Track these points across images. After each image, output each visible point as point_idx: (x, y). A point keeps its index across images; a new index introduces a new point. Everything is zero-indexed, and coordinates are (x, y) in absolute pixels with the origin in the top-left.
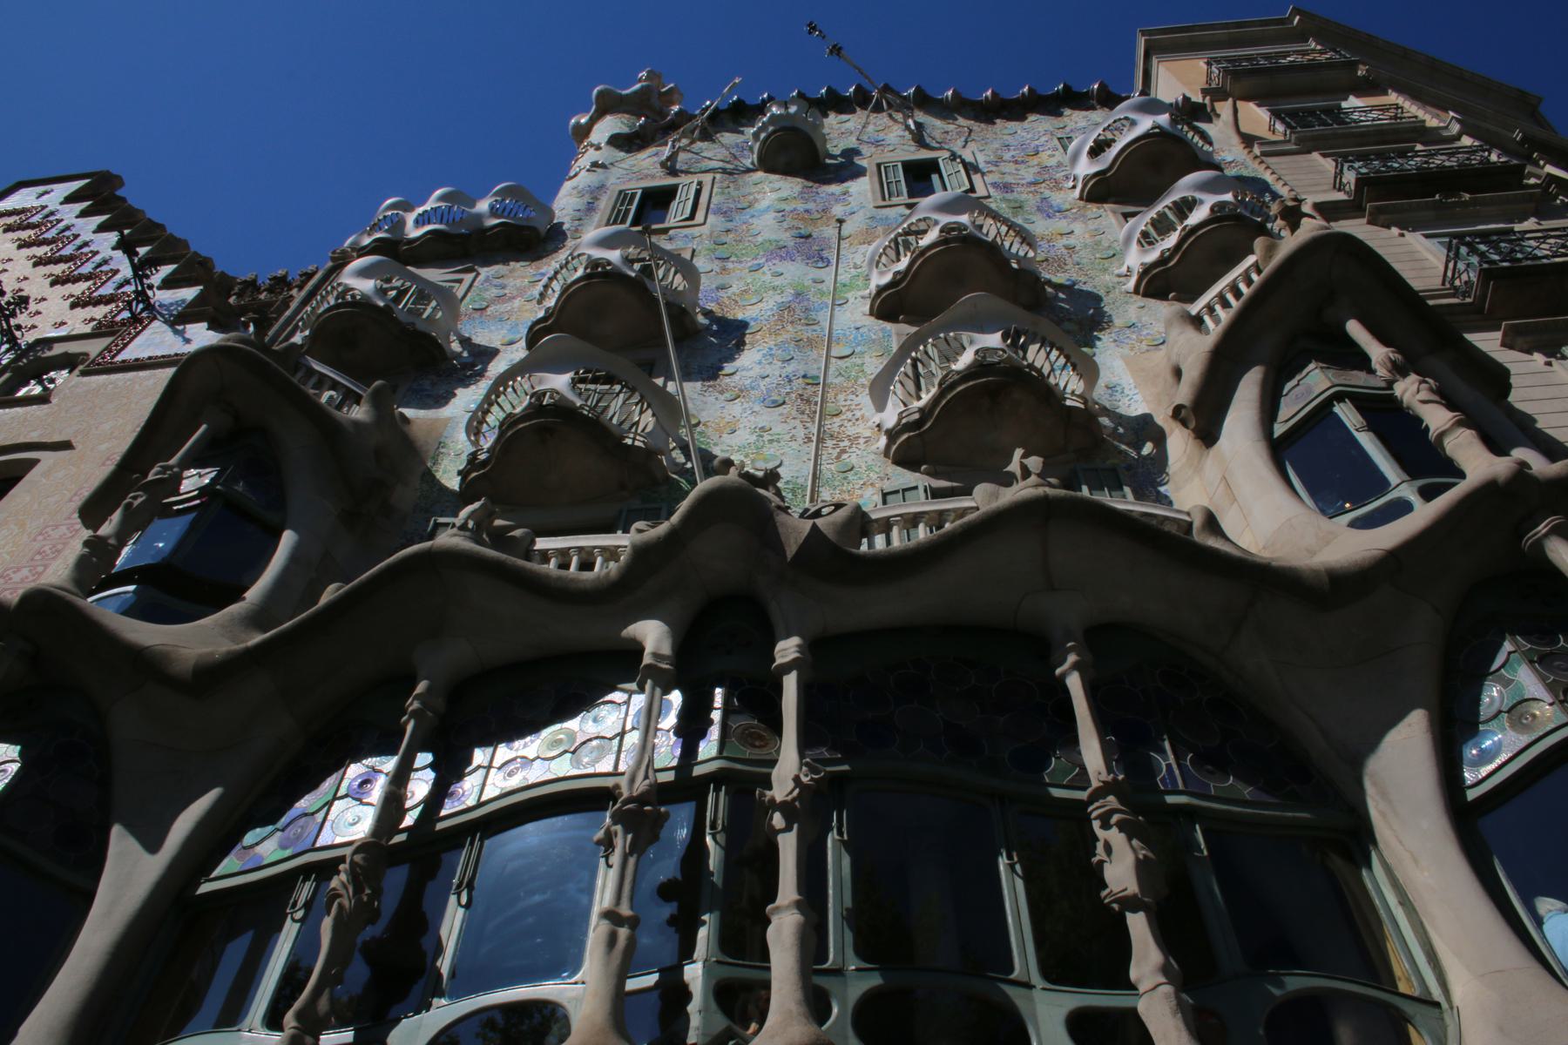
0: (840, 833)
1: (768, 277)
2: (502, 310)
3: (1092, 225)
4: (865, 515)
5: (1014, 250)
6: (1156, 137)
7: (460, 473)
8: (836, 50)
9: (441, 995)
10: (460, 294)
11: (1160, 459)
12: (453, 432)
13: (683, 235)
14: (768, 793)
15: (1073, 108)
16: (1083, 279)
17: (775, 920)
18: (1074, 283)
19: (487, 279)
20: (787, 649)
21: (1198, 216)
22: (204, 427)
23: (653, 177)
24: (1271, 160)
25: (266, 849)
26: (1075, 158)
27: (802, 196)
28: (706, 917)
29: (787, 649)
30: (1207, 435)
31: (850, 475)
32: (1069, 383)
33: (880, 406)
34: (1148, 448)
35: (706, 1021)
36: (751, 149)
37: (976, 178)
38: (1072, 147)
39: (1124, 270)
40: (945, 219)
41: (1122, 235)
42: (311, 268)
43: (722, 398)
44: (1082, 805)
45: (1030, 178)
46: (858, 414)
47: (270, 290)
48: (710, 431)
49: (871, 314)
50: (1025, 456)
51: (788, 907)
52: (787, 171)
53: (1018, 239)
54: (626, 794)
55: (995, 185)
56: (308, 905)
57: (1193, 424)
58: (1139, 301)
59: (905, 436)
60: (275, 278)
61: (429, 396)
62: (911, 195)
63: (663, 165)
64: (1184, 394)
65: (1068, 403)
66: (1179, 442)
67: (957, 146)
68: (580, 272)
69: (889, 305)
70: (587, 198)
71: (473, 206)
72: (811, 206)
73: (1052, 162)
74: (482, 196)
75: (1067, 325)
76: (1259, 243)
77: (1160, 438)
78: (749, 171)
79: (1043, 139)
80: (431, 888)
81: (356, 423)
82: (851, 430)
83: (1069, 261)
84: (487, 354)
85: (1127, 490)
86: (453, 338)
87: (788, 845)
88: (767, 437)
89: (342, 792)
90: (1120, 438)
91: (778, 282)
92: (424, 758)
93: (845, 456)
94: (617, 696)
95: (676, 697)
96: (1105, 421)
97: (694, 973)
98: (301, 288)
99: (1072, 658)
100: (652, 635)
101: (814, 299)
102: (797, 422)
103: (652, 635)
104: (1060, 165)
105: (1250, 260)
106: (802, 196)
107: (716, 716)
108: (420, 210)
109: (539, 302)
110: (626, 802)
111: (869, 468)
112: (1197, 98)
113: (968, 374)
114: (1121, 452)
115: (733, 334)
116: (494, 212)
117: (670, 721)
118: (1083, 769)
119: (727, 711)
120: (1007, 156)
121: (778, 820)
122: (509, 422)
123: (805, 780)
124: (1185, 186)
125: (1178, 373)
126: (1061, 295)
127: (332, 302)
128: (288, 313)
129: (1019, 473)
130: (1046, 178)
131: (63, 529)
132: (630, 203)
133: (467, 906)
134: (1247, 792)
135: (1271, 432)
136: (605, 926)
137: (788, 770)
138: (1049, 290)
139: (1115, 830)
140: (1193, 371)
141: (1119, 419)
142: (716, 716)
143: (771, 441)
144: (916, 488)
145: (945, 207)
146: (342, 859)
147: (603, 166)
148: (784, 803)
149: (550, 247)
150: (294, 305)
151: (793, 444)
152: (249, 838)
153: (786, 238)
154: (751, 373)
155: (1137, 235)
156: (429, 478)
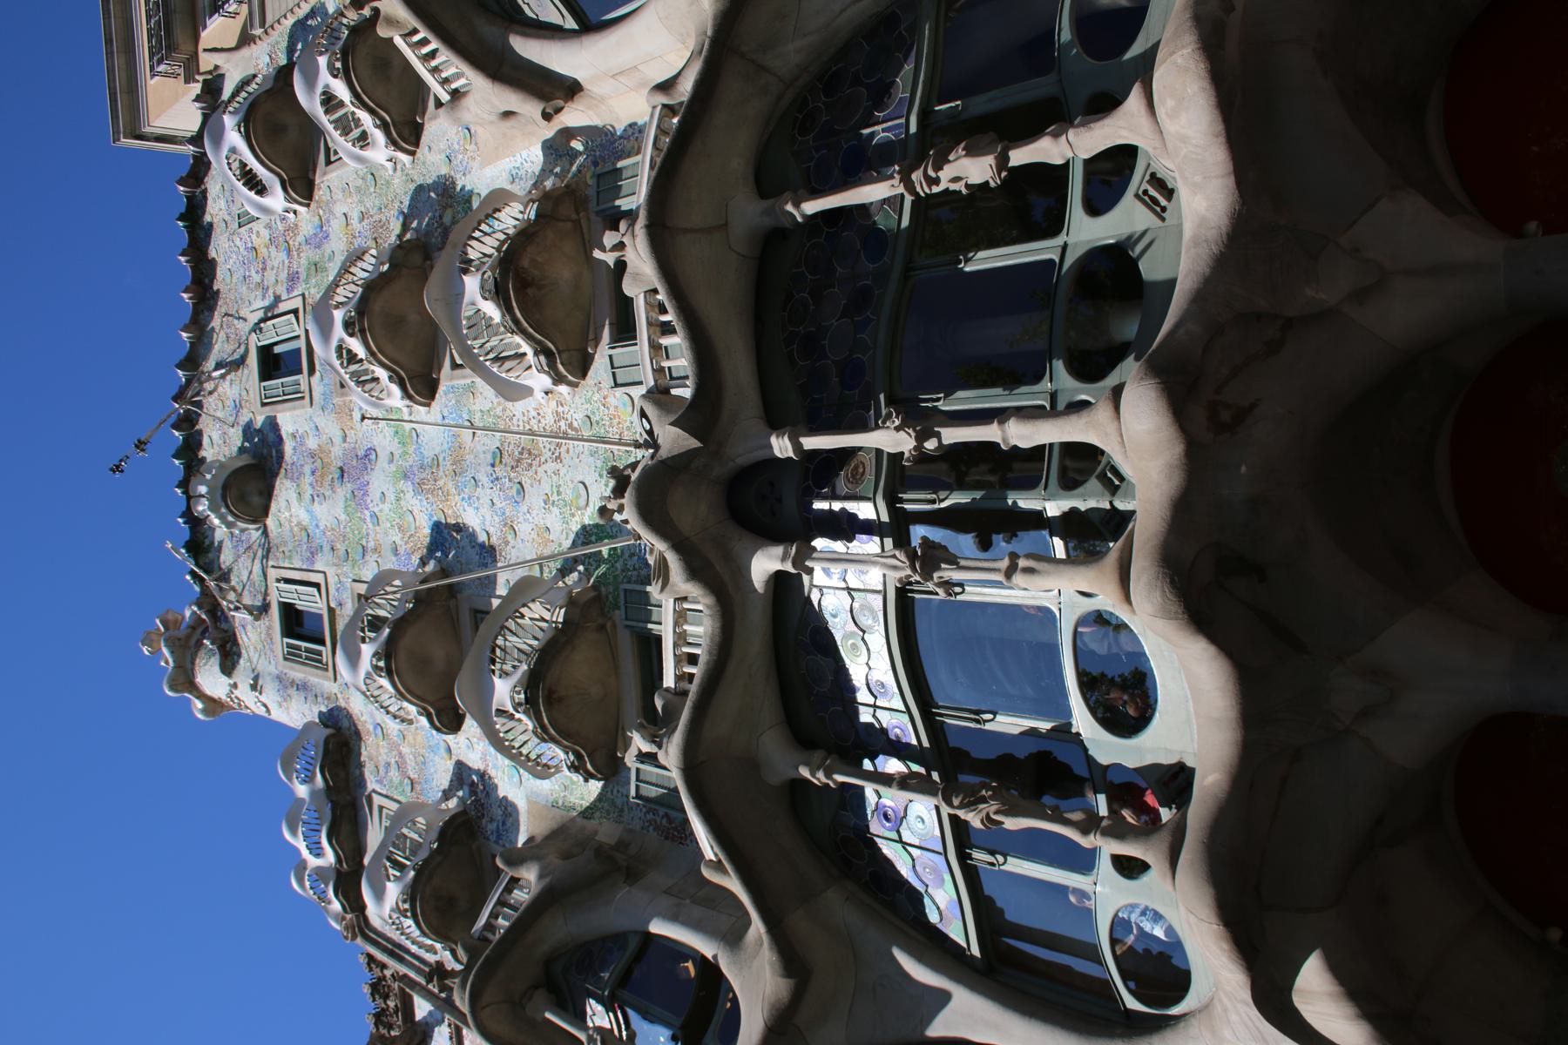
0: (938, 400)
1: (386, 507)
2: (415, 764)
3: (338, 195)
4: (649, 392)
5: (370, 268)
6: (248, 127)
7: (586, 780)
8: (140, 445)
9: (1070, 725)
10: (394, 806)
11: (588, 132)
12: (543, 790)
13: (337, 590)
14: (907, 455)
15: (204, 212)
16: (397, 205)
17: (1014, 442)
19: (380, 782)
20: (781, 447)
21: (341, 90)
22: (548, 1015)
23: (269, 628)
24: (269, 19)
25: (944, 902)
26: (265, 210)
27: (296, 478)
28: (1010, 502)
29: (781, 447)
30: (571, 89)
31: (594, 419)
32: (510, 219)
33: (528, 391)
34: (577, 145)
35: (1092, 495)
36: (243, 531)
37: (283, 307)
39: (389, 165)
40: (339, 332)
41: (352, 164)
42: (362, 960)
43: (512, 542)
44: (918, 202)
45: (283, 256)
46: (533, 413)
47: (386, 997)
49: (428, 405)
50: (603, 249)
51: (1003, 431)
52: (268, 494)
53: (360, 264)
54: (909, 572)
55: (289, 291)
56: (992, 853)
57: (560, 103)
58: (422, 151)
59: (560, 367)
60: (372, 994)
61: (504, 823)
62: (300, 372)
63: (257, 618)
64: (530, 108)
65: (532, 216)
66: (574, 116)
67: (244, 328)
68: (385, 682)
69: (422, 386)
70: (292, 691)
71: (303, 800)
72: (307, 470)
73: (265, 233)
74: (291, 792)
75: (447, 219)
76: (383, 31)
77: (568, 133)
78: (265, 533)
79: (238, 242)
80: (979, 753)
81: (541, 877)
83: (377, 218)
84: (462, 772)
85: (619, 165)
86: (443, 806)
87: (953, 435)
88: (555, 497)
89: (894, 835)
90: (565, 171)
91: (391, 497)
92: (867, 765)
93: (575, 424)
94: (815, 596)
95: (820, 543)
96: (548, 184)
97: (1053, 509)
98: (384, 966)
99: (789, 208)
100: (765, 564)
101: (411, 460)
103: (765, 564)
106: (296, 478)
107: (837, 506)
108: (305, 853)
109: (411, 722)
110: (914, 569)
111: (589, 401)
112: (197, 88)
113: (507, 308)
114: (579, 171)
115: (445, 536)
116: (308, 780)
117: (839, 546)
118: (885, 201)
119: (834, 497)
120: (257, 278)
121: (931, 445)
122: (544, 735)
123: (897, 423)
124: (310, 103)
125: (508, 114)
126: (414, 225)
127: (410, 922)
128: (412, 975)
129: (617, 254)
130: (284, 240)
132: (299, 648)
133: (995, 714)
134: (908, 67)
135: (574, 31)
136: (1018, 579)
137: (892, 439)
138: (408, 236)
139: (941, 174)
140: (510, 99)
141: (545, 171)
142: (837, 506)
143: (559, 493)
145: (326, 332)
146: (954, 819)
147: (256, 679)
148: (917, 439)
149: (345, 723)
150: (403, 970)
152: (933, 917)
153: (343, 491)
154: (488, 517)
155: (357, 150)
156: (587, 813)
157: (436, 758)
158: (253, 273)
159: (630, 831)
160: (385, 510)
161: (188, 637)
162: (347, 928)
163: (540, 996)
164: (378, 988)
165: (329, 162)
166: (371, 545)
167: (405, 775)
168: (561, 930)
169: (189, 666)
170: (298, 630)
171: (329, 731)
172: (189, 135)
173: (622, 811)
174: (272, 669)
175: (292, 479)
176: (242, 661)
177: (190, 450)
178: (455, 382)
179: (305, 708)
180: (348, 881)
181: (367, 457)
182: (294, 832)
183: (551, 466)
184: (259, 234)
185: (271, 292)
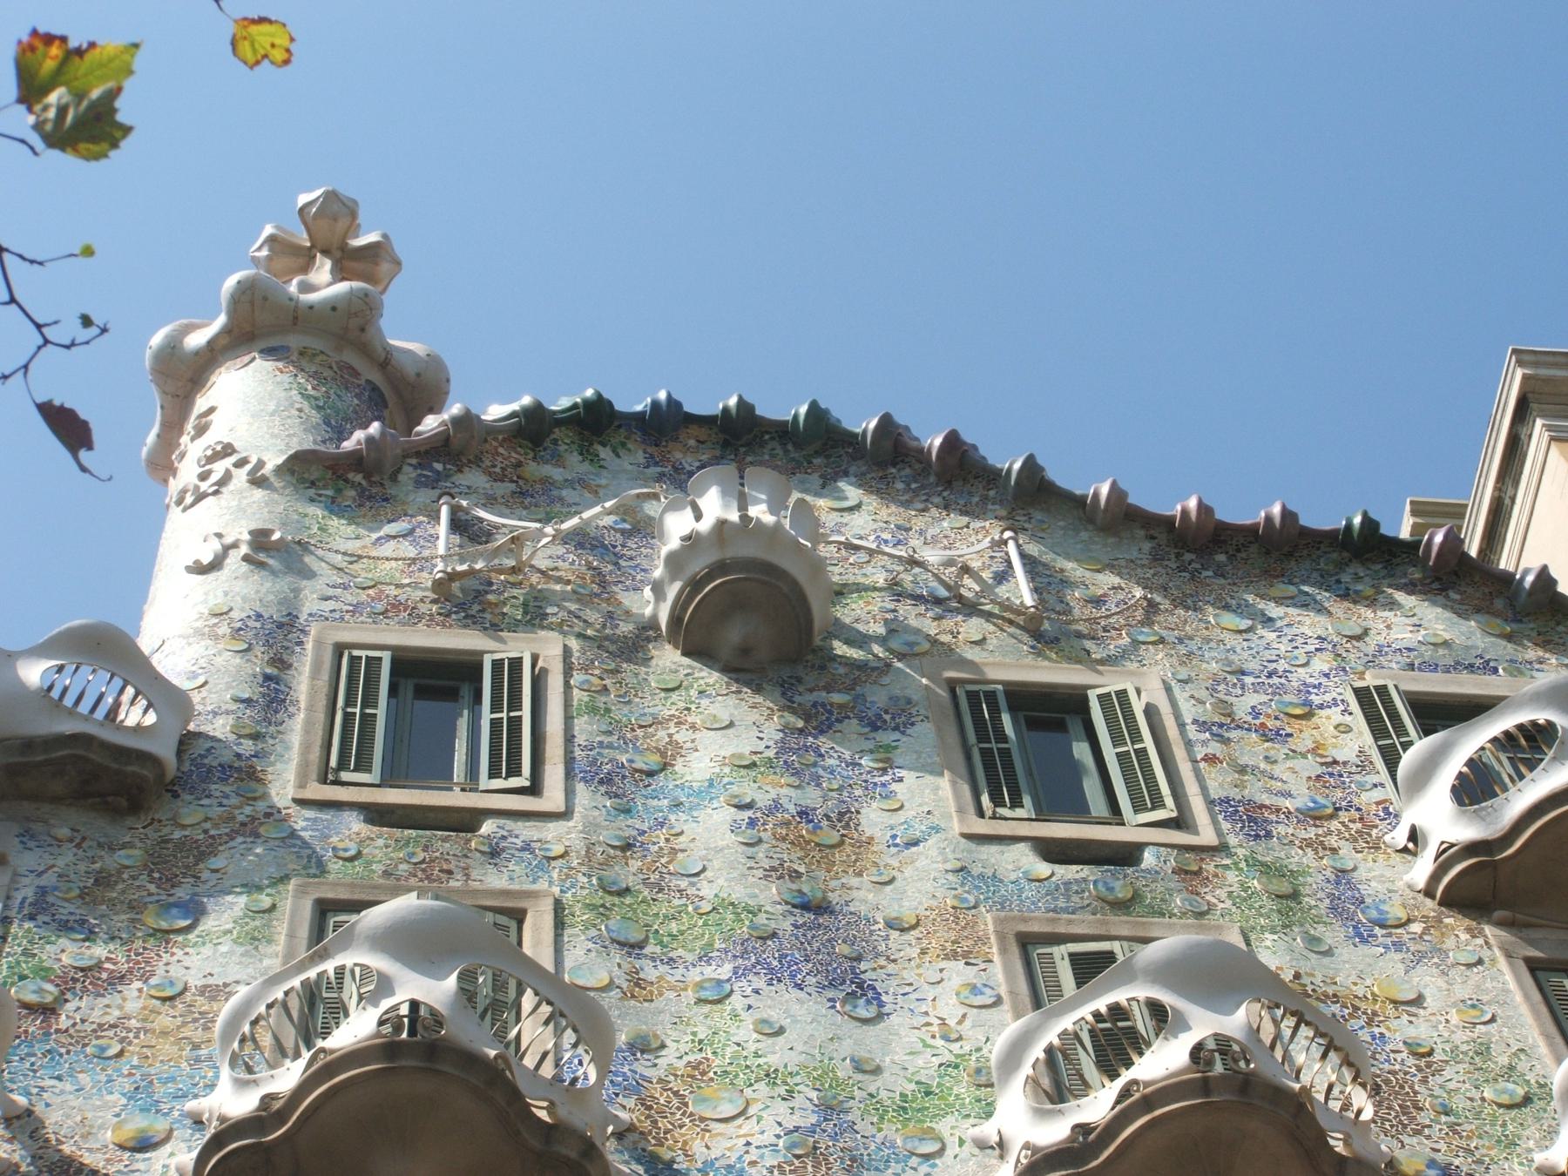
1: (745, 1032)
45: (1302, 797)
52: (744, 670)
70: (258, 664)
72: (810, 796)
79: (1321, 664)
83: (1424, 1099)
91: (777, 1055)
104: (1364, 765)
120: (1243, 705)
132: (370, 700)
158: (1253, 699)
161: (365, 349)
165: (1534, 966)
166: (650, 972)
169: (294, 341)
174: (310, 603)
175: (783, 748)
176: (316, 511)
181: (855, 989)
185: (1215, 748)
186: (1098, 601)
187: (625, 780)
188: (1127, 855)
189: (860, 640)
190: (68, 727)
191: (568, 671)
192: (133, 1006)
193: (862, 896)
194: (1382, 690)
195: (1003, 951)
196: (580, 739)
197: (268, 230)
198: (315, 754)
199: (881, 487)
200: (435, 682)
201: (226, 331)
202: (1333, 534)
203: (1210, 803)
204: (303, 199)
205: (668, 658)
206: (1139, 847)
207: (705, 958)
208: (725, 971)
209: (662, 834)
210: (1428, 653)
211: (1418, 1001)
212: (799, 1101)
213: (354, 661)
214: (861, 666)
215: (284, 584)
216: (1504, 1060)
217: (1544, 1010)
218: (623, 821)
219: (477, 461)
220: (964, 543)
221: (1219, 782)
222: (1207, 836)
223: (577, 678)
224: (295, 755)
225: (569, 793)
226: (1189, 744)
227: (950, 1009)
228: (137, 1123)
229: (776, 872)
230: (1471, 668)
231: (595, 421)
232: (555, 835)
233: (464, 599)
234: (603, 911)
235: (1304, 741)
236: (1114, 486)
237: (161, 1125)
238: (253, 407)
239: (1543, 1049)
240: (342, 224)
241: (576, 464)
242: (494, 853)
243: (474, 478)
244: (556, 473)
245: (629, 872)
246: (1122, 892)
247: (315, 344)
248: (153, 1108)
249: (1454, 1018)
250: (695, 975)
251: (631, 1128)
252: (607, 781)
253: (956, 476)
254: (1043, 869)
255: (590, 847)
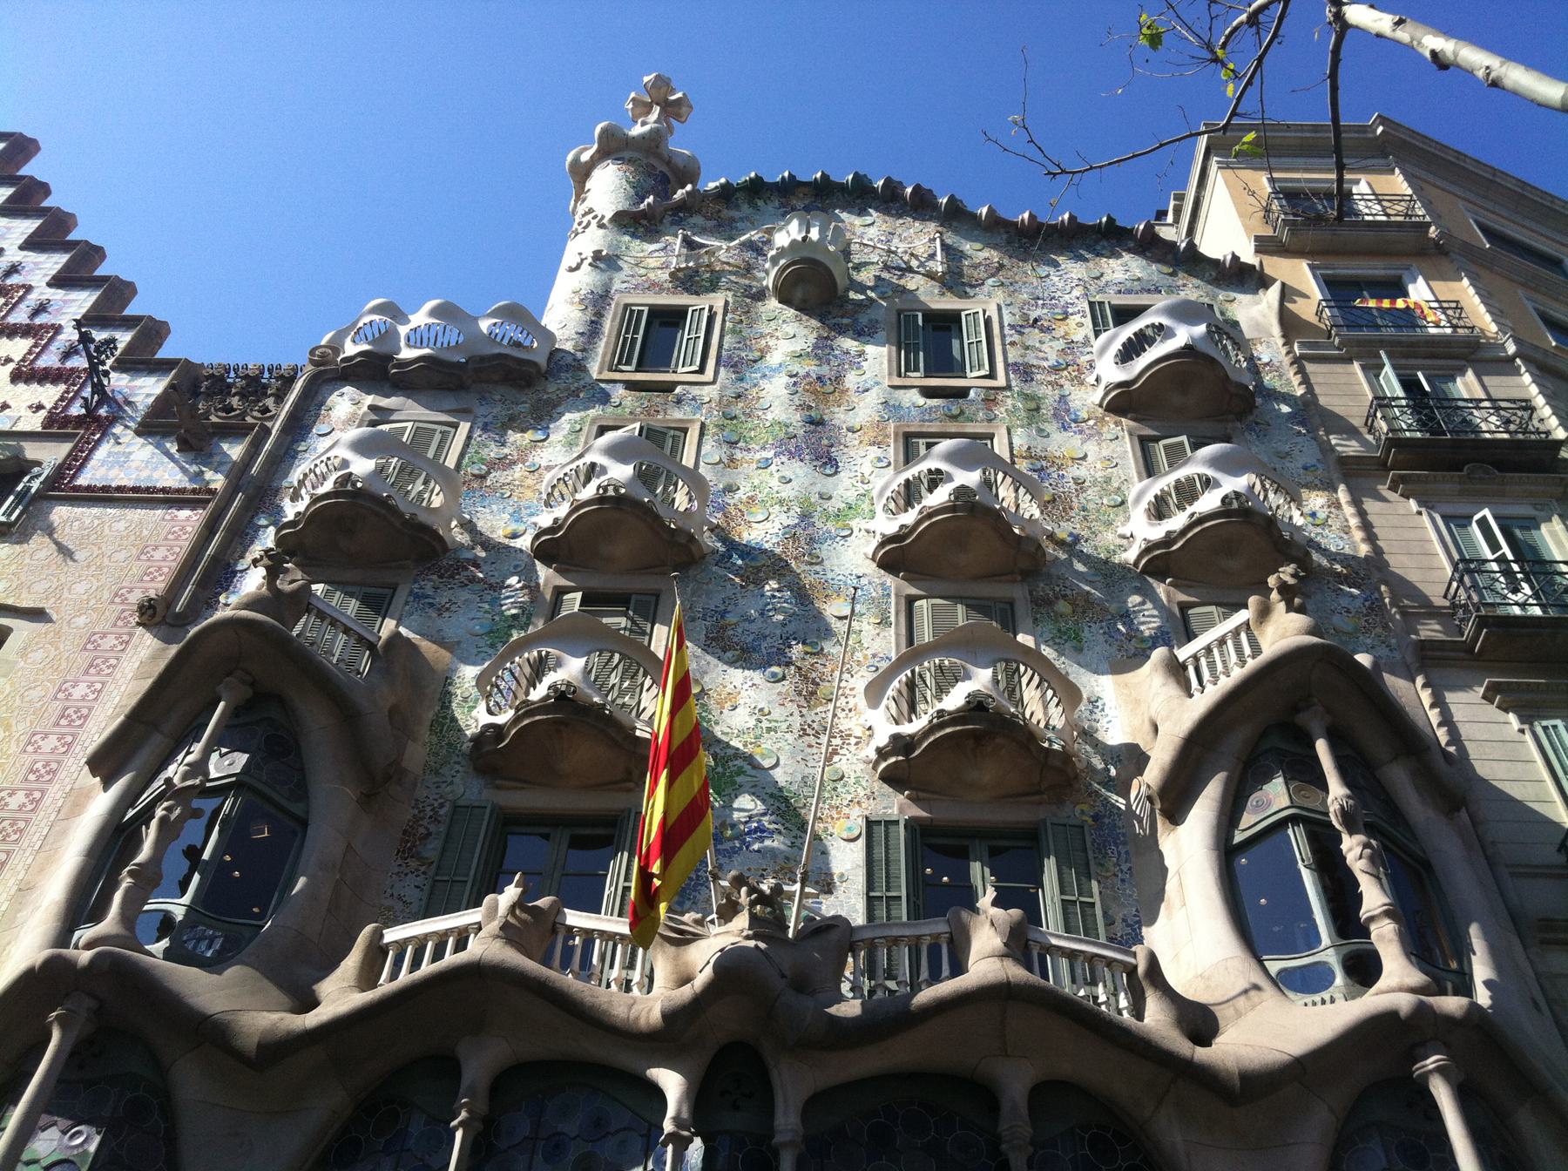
1: (774, 483)
18: (1077, 539)
21: (1209, 502)
24: (1310, 367)
31: (839, 785)
38: (1104, 337)
45: (1052, 362)
46: (852, 702)
47: (243, 395)
48: (712, 704)
49: (873, 559)
52: (804, 308)
59: (893, 760)
61: (431, 605)
68: (589, 492)
70: (589, 316)
73: (1078, 336)
76: (1253, 600)
82: (844, 724)
83: (1075, 505)
86: (454, 523)
88: (765, 724)
91: (787, 492)
93: (836, 758)
98: (280, 398)
102: (793, 707)
104: (1086, 343)
105: (1242, 616)
112: (1248, 256)
113: (957, 717)
125: (1156, 729)
131: (53, 741)
132: (636, 331)
143: (769, 730)
144: (897, 822)
150: (276, 427)
151: (788, 736)
157: (506, 516)
159: (415, 784)
160: (770, 481)
161: (659, 156)
162: (323, 356)
163: (247, 692)
164: (255, 386)
166: (739, 455)
167: (493, 465)
168: (316, 723)
169: (627, 155)
170: (656, 323)
171: (542, 360)
172: (1197, 241)
173: (437, 773)
174: (617, 285)
175: (816, 347)
176: (627, 238)
177: (860, 196)
178: (893, 600)
179: (570, 332)
180: (375, 371)
182: (434, 313)
183: (797, 721)
184: (1078, 325)
185: (1016, 338)
186: (975, 266)
187: (741, 364)
188: (962, 393)
189: (861, 288)
190: (497, 351)
191: (725, 314)
192: (517, 475)
193: (839, 417)
194: (1101, 303)
195: (896, 441)
196: (726, 346)
197: (633, 95)
198: (608, 358)
199: (886, 211)
200: (668, 320)
201: (598, 151)
202: (1093, 226)
203: (1007, 365)
204: (646, 79)
205: (773, 303)
206: (969, 388)
207: (763, 448)
208: (770, 454)
209: (755, 390)
210: (1129, 284)
211: (1084, 458)
212: (792, 513)
213: (632, 312)
214: (859, 304)
215: (605, 276)
216: (1116, 485)
217: (1141, 461)
218: (740, 384)
219: (699, 212)
220: (919, 240)
221: (1014, 354)
222: (1001, 381)
223: (729, 316)
224: (599, 359)
225: (716, 373)
226: (1003, 336)
227: (867, 469)
228: (513, 527)
229: (804, 407)
230: (1149, 291)
231: (756, 189)
232: (709, 393)
233: (687, 281)
234: (722, 427)
235: (1059, 332)
236: (990, 210)
237: (521, 528)
238: (608, 188)
239: (1136, 479)
240: (664, 90)
241: (746, 209)
242: (679, 401)
243: (698, 220)
244: (735, 214)
245: (737, 409)
246: (955, 411)
247: (636, 155)
248: (519, 520)
249: (1099, 466)
250: (758, 456)
251: (718, 526)
252: (735, 366)
253: (921, 205)
254: (921, 401)
255: (722, 397)
